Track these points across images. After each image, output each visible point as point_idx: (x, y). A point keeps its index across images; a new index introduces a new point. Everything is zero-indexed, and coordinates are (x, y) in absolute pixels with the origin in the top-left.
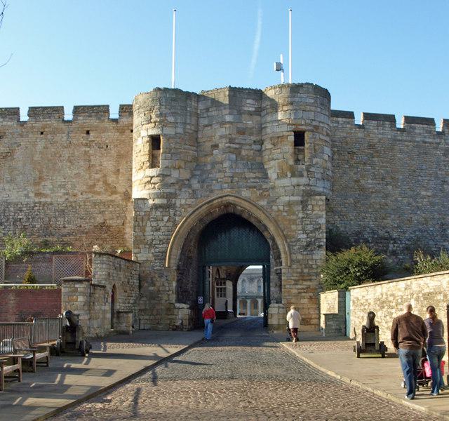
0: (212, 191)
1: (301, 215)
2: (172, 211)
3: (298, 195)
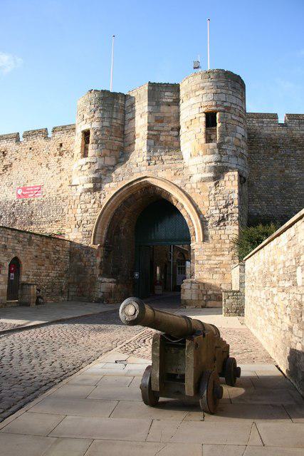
0: (132, 174)
1: (213, 192)
2: (97, 194)
3: (210, 171)
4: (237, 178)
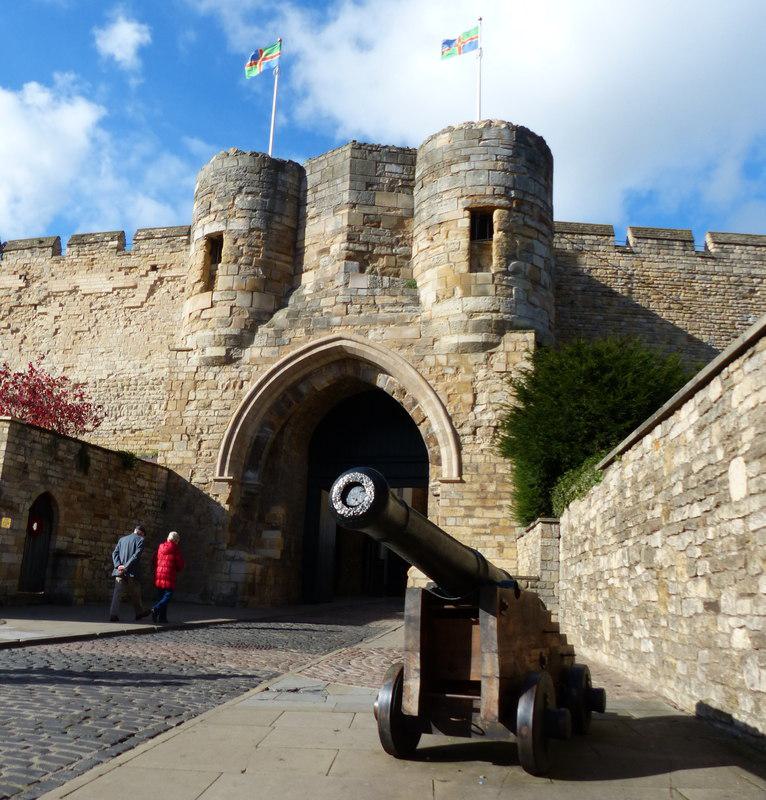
1: (481, 373)
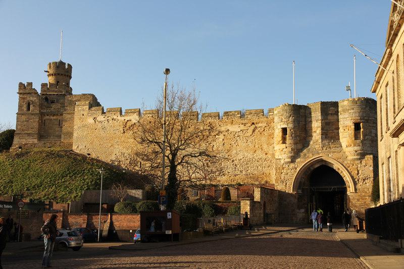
4: (372, 159)
